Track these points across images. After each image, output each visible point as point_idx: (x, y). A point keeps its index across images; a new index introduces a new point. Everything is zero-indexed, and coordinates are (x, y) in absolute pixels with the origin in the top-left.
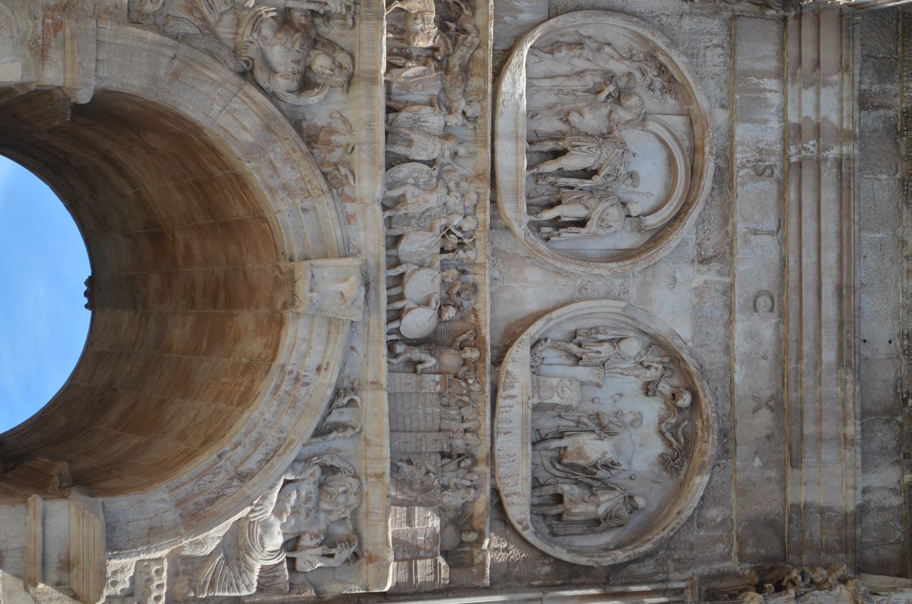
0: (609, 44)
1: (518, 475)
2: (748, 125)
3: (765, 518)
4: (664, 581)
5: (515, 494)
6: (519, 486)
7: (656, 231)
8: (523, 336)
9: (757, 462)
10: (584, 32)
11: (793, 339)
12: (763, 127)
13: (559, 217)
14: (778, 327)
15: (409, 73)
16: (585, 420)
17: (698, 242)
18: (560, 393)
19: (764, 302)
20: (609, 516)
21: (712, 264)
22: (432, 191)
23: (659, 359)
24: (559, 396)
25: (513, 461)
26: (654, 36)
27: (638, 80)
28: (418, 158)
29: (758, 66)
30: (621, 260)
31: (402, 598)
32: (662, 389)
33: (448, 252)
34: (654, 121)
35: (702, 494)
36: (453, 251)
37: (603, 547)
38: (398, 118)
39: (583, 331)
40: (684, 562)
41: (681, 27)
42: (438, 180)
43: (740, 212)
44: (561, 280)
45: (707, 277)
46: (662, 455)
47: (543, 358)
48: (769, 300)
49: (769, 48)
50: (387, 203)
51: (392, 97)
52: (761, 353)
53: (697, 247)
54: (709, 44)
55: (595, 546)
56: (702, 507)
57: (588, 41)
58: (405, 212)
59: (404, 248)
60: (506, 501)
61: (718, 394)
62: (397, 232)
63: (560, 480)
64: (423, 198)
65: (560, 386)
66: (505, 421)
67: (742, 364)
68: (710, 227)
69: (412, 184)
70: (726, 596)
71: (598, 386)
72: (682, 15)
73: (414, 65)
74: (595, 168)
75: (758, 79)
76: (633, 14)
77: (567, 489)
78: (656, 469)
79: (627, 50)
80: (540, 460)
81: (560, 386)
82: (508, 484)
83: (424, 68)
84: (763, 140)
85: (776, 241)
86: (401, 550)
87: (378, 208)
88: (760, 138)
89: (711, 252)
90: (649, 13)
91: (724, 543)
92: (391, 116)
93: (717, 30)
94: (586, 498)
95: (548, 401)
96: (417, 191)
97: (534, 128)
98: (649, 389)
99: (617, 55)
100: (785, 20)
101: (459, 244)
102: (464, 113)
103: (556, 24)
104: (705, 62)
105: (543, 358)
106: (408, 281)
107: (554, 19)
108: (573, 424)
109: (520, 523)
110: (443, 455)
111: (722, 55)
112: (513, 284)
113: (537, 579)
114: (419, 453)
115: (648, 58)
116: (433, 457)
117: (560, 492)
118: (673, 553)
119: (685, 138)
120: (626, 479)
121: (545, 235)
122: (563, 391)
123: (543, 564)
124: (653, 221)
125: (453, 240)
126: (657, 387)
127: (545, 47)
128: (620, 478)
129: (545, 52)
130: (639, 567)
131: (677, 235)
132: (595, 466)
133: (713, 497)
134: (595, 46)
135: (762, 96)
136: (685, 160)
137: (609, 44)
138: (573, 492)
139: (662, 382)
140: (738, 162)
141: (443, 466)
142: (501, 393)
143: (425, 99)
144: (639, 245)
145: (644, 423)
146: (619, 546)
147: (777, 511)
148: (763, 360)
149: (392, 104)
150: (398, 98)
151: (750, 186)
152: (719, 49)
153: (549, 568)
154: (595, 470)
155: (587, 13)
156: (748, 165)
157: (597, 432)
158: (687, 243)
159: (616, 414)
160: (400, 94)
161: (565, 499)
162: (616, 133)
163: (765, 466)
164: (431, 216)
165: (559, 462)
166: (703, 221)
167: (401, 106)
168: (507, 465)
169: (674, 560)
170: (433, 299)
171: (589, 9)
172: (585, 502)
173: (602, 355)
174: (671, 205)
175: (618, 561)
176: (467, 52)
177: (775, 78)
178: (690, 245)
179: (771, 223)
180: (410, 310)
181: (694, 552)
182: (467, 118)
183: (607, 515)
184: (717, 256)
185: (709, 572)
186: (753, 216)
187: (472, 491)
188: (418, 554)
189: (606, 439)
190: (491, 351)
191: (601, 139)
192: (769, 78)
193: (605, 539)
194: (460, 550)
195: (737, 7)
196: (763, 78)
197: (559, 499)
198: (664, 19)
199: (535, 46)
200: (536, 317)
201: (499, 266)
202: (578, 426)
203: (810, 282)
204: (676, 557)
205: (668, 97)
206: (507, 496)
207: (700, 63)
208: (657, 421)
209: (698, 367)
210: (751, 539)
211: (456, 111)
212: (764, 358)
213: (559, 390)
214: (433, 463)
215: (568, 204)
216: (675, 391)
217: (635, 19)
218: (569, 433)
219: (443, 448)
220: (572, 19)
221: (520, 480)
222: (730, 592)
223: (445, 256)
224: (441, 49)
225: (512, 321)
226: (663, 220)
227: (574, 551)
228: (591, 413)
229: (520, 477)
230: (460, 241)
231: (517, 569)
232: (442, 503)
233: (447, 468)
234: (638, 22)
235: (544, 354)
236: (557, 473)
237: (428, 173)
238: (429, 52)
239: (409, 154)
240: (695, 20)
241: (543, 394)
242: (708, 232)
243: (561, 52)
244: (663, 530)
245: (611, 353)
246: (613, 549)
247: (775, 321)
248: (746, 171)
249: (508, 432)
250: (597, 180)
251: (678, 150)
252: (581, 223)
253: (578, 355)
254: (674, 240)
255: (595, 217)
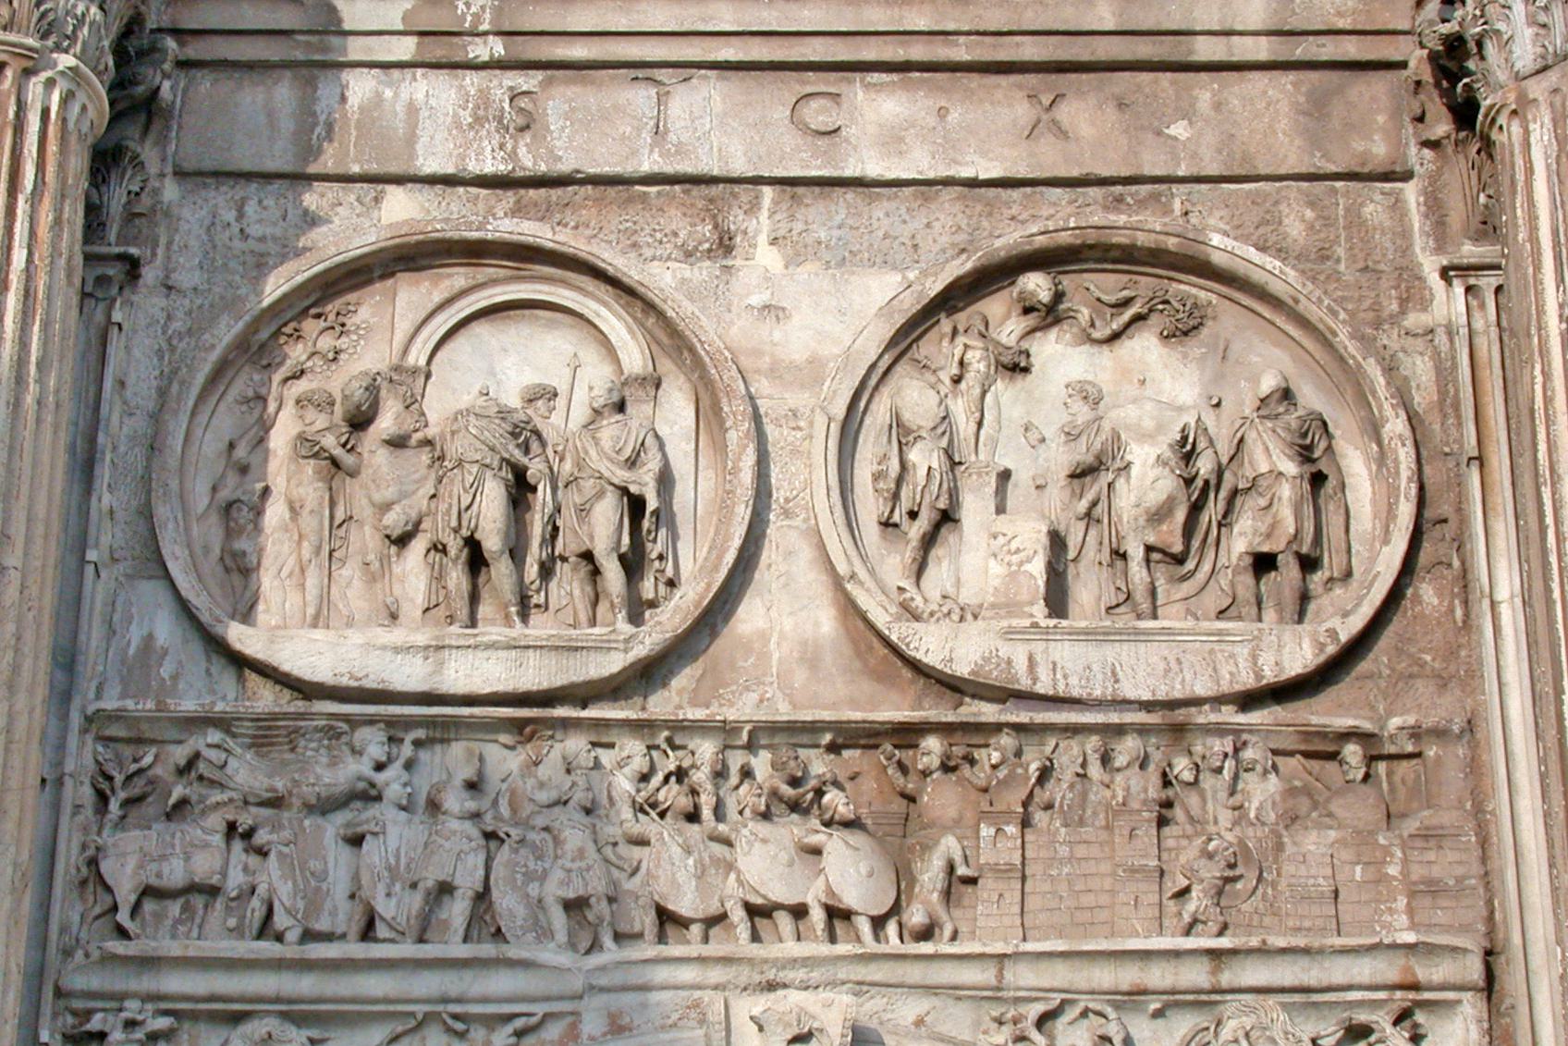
0: (232, 446)
1: (1211, 652)
2: (420, 148)
3: (1304, 113)
4: (1451, 334)
5: (1254, 658)
6: (1238, 649)
7: (654, 347)
8: (894, 638)
9: (1179, 130)
10: (200, 497)
11: (901, 52)
12: (424, 113)
13: (622, 558)
14: (875, 85)
15: (284, 891)
16: (1083, 506)
17: (680, 255)
18: (1022, 555)
19: (817, 114)
20: (1305, 454)
21: (732, 227)
22: (557, 841)
23: (945, 343)
24: (1029, 560)
25: (1179, 662)
26: (213, 346)
27: (314, 385)
28: (481, 872)
29: (287, 125)
30: (721, 422)
31: (1498, 916)
32: (1014, 337)
33: (697, 807)
34: (405, 351)
35: (1252, 249)
36: (694, 792)
37: (1374, 467)
38: (388, 916)
39: (881, 508)
40: (1408, 290)
41: (195, 289)
42: (533, 828)
43: (616, 165)
44: (768, 555)
45: (763, 239)
46: (1166, 337)
47: (944, 597)
48: (815, 104)
49: (249, 99)
50: (585, 944)
51: (339, 931)
52: (932, 121)
53: (693, 259)
54: (235, 229)
55: (1373, 485)
56: (1280, 250)
57: (225, 494)
58: (604, 903)
59: (684, 905)
60: (1270, 676)
61: (1024, 216)
62: (648, 921)
63: (1223, 560)
64: (573, 860)
65: (1007, 559)
66: (1088, 679)
67: (955, 162)
68: (647, 231)
69: (541, 885)
70: (1482, 199)
71: (1005, 476)
72: (170, 288)
73: (265, 878)
74: (510, 476)
75: (315, 124)
76: (163, 393)
77: (1242, 539)
78: (1198, 352)
79: (244, 408)
80: (1177, 605)
81: (1007, 559)
82: (1231, 674)
83: (273, 856)
84: (455, 115)
85: (682, 88)
86: (1387, 918)
87: (596, 960)
88: (449, 119)
89: (707, 229)
90: (161, 358)
91: (1362, 205)
92: (382, 931)
93: (203, 213)
94: (1263, 502)
95: (1041, 583)
96: (557, 875)
97: (419, 612)
98: (1017, 367)
99: (254, 430)
100: (184, 64)
101: (679, 781)
102: (380, 767)
103: (181, 561)
104: (274, 239)
105: (944, 597)
106: (764, 897)
107: (170, 565)
108: (1093, 533)
109: (1322, 646)
110: (1162, 822)
111: (260, 202)
112: (774, 663)
113: (1452, 610)
114: (1162, 873)
115: (264, 362)
116: (1170, 843)
117: (1248, 560)
118: (1385, 314)
119: (447, 283)
120: (1218, 417)
121: (662, 589)
122: (1018, 551)
123: (1417, 599)
124: (634, 358)
125: (672, 795)
126: (1010, 348)
127: (233, 587)
128: (1221, 431)
129: (246, 587)
130: (1418, 386)
131: (665, 301)
132: (1189, 482)
133: (1257, 227)
134: (232, 479)
135: (356, 116)
136: (494, 282)
137: (232, 446)
138: (1249, 531)
139: (998, 338)
140: (502, 167)
141: (1191, 819)
142: (1024, 683)
143: (346, 852)
144: (687, 386)
145: (1090, 378)
146: (1374, 429)
147: (1289, 87)
148: (949, 118)
149: (355, 928)
150: (341, 917)
151: (558, 144)
152: (246, 208)
153: (1424, 585)
154: (1199, 483)
155: (157, 493)
156: (509, 146)
157: (1110, 476)
158: (683, 280)
159: (1071, 436)
160: (334, 913)
161: (1265, 549)
162: (431, 432)
163: (1188, 114)
164: (615, 844)
165: (1179, 560)
166: (635, 245)
167: (359, 909)
168: (1188, 676)
169: (1403, 312)
170: (806, 840)
171: (149, 492)
172: (1270, 504)
173: (935, 465)
174: (598, 315)
175: (1407, 433)
176: (239, 758)
177: (315, 89)
178: (688, 274)
179: (640, 98)
180: (830, 892)
181: (1382, 267)
182: (390, 760)
183: (1301, 455)
184: (714, 217)
185: (1429, 235)
186: (623, 137)
187: (1248, 754)
188: (1394, 878)
189: (1128, 457)
190: (924, 709)
191: (446, 463)
192: (315, 100)
193: (1355, 464)
194: (1385, 785)
195: (153, 168)
196: (314, 114)
197: (1263, 563)
198: (177, 325)
199: (231, 610)
200: (850, 610)
201: (733, 692)
202: (1098, 521)
203: (775, 14)
204: (1395, 307)
205: (351, 321)
206: (1259, 676)
207: (278, 249)
208: (1086, 348)
209: (964, 256)
210: (1354, 145)
211: (373, 785)
212: (942, 113)
213: (1015, 559)
214: (1184, 842)
215: (592, 538)
216: (1018, 309)
217: (175, 388)
218: (1114, 539)
219: (1149, 821)
220: (171, 526)
221: (1224, 646)
222: (1475, 190)
223: (707, 813)
224: (230, 817)
225: (857, 664)
226: (630, 331)
227: (1387, 531)
228: (1068, 492)
229: (1216, 646)
230: (673, 779)
231: (1428, 658)
232: (1277, 824)
233: (1195, 812)
234: (182, 383)
235: (934, 593)
236: (1206, 567)
237: (516, 851)
238: (238, 845)
239: (470, 893)
240: (181, 260)
241: (1024, 597)
242: (658, 236)
243: (244, 553)
244: (1335, 334)
245: (930, 445)
246: (1380, 444)
247: (860, 95)
248: (522, 151)
249: (1114, 673)
250: (535, 469)
251: (472, 298)
252: (636, 505)
253: (936, 516)
254: (680, 307)
255: (621, 476)
